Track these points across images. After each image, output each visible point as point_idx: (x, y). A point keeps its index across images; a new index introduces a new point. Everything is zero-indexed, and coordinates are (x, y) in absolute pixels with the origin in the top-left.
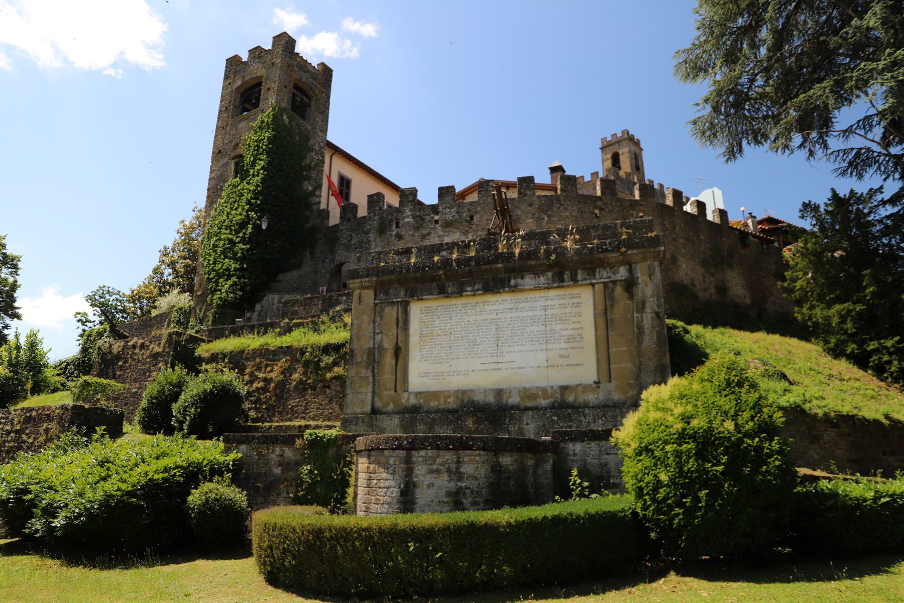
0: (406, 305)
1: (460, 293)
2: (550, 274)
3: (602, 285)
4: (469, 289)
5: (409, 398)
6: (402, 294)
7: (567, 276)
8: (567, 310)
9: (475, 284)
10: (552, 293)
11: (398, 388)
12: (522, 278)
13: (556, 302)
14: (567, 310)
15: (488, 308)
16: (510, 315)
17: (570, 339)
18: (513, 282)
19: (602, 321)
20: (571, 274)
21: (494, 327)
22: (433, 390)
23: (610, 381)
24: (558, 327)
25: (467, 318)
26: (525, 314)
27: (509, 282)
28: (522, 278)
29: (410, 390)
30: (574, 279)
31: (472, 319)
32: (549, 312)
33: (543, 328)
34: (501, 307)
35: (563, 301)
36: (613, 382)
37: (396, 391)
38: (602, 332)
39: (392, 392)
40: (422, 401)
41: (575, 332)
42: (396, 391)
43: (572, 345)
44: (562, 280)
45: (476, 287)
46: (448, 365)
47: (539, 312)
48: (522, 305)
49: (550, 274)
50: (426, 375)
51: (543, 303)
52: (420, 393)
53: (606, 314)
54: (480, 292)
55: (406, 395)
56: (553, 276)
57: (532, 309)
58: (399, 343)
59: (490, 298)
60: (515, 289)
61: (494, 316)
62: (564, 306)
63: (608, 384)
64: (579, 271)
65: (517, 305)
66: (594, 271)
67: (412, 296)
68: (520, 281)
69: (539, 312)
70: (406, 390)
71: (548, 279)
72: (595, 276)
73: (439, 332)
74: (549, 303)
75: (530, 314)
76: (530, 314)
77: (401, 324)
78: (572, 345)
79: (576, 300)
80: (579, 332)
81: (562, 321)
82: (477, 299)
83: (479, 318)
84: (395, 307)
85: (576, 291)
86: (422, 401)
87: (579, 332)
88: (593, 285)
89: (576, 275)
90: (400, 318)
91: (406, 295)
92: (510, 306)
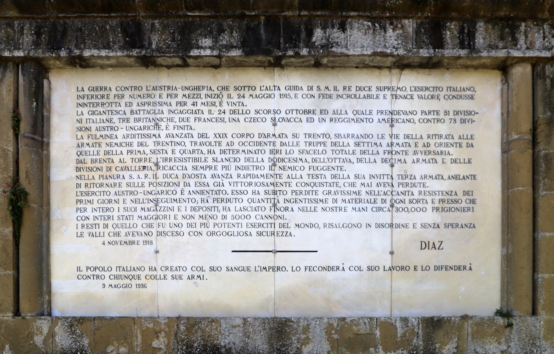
0: (39, 72)
1: (183, 58)
2: (410, 25)
3: (528, 68)
4: (207, 42)
5: (52, 334)
6: (28, 39)
7: (451, 32)
8: (443, 129)
9: (221, 31)
10: (410, 80)
11: (24, 305)
12: (343, 28)
13: (418, 105)
14: (443, 129)
15: (252, 104)
16: (307, 127)
17: (447, 203)
18: (318, 34)
19: (524, 161)
20: (461, 32)
21: (267, 156)
22: (114, 314)
23: (534, 312)
24: (419, 170)
25: (199, 127)
26: (342, 128)
27: (310, 34)
28: (343, 28)
29: (56, 312)
30: (467, 40)
31: (211, 129)
32: (401, 129)
33: (385, 169)
34: (285, 105)
35: (433, 105)
36: (543, 315)
37: (17, 312)
38: (524, 188)
39: (8, 316)
40: (86, 342)
41: (458, 186)
42: (17, 312)
43: (451, 218)
44: (439, 44)
45: (225, 39)
46: (151, 249)
47: (376, 128)
48: (336, 104)
49: (410, 25)
50: (94, 272)
51: (385, 104)
52: (81, 320)
53: (534, 143)
54: (235, 53)
55: (44, 325)
56: (417, 32)
57: (360, 117)
58: (23, 181)
59: (260, 79)
60: (324, 61)
61: (267, 127)
62: (432, 117)
63: (531, 320)
64: (481, 26)
65: (325, 104)
66: (514, 30)
67: (55, 45)
68: (336, 34)
69: (376, 128)
70: (45, 310)
71: (404, 37)
72: (515, 42)
73: (127, 158)
74: (401, 105)
75: (356, 129)
76: (356, 129)
77: (25, 127)
78: (451, 218)
79: (464, 105)
80: (467, 185)
81: (430, 154)
82: (227, 78)
83: (229, 128)
84: (9, 77)
85: (465, 81)
86: (86, 342)
87: (467, 185)
88: (504, 67)
89: (472, 35)
90: (22, 110)
91: (36, 44)
92: (308, 104)
